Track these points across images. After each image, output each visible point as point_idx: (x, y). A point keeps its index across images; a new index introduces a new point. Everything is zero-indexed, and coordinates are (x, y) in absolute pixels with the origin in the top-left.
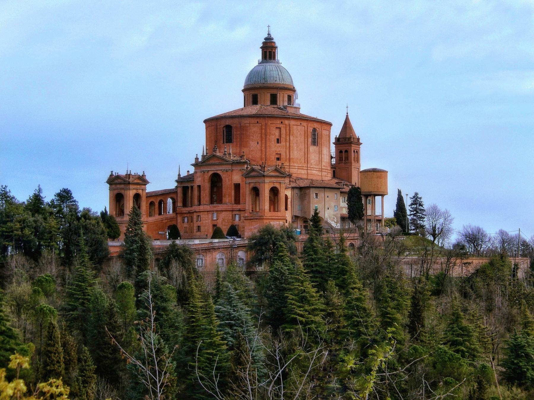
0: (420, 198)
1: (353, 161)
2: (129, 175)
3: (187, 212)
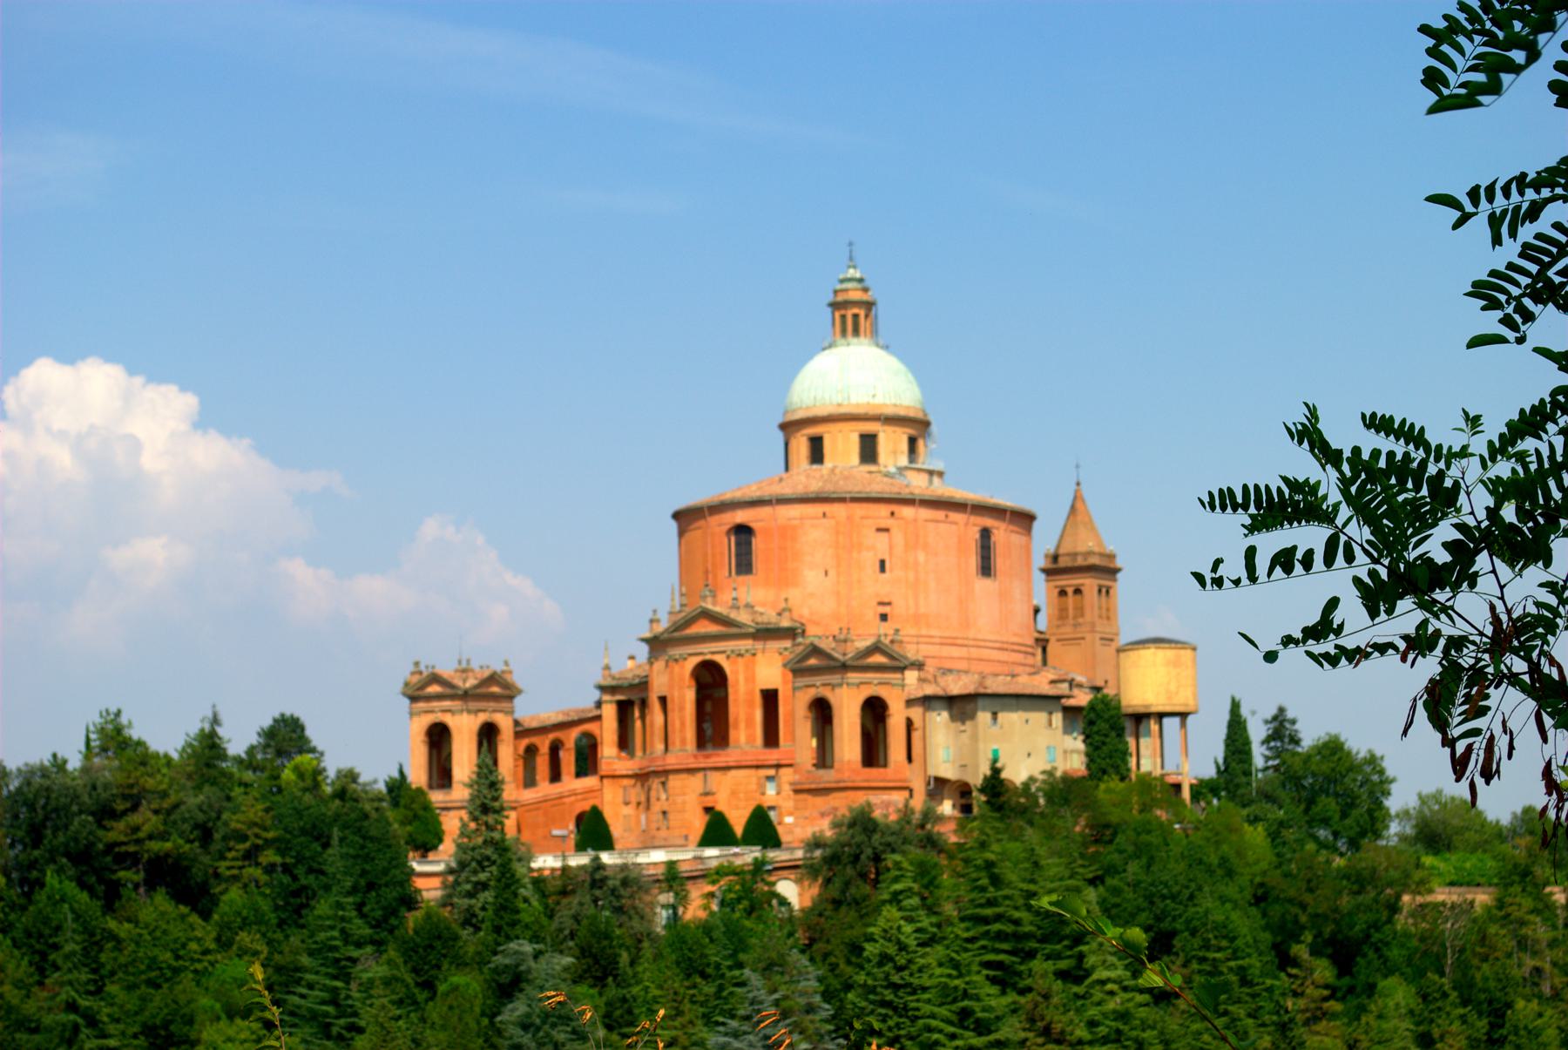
0: (1293, 722)
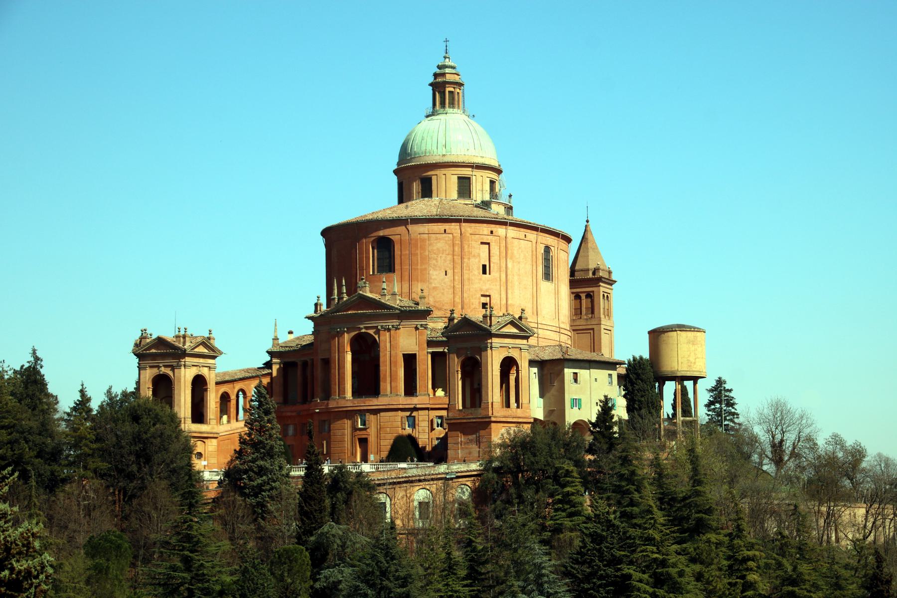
0: (730, 391)
1: (602, 316)
2: (184, 337)
3: (294, 414)
